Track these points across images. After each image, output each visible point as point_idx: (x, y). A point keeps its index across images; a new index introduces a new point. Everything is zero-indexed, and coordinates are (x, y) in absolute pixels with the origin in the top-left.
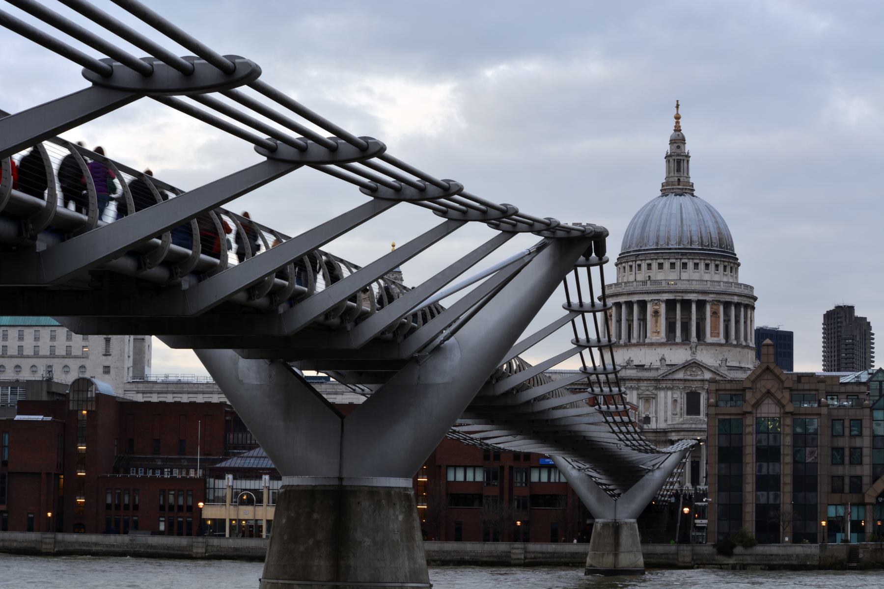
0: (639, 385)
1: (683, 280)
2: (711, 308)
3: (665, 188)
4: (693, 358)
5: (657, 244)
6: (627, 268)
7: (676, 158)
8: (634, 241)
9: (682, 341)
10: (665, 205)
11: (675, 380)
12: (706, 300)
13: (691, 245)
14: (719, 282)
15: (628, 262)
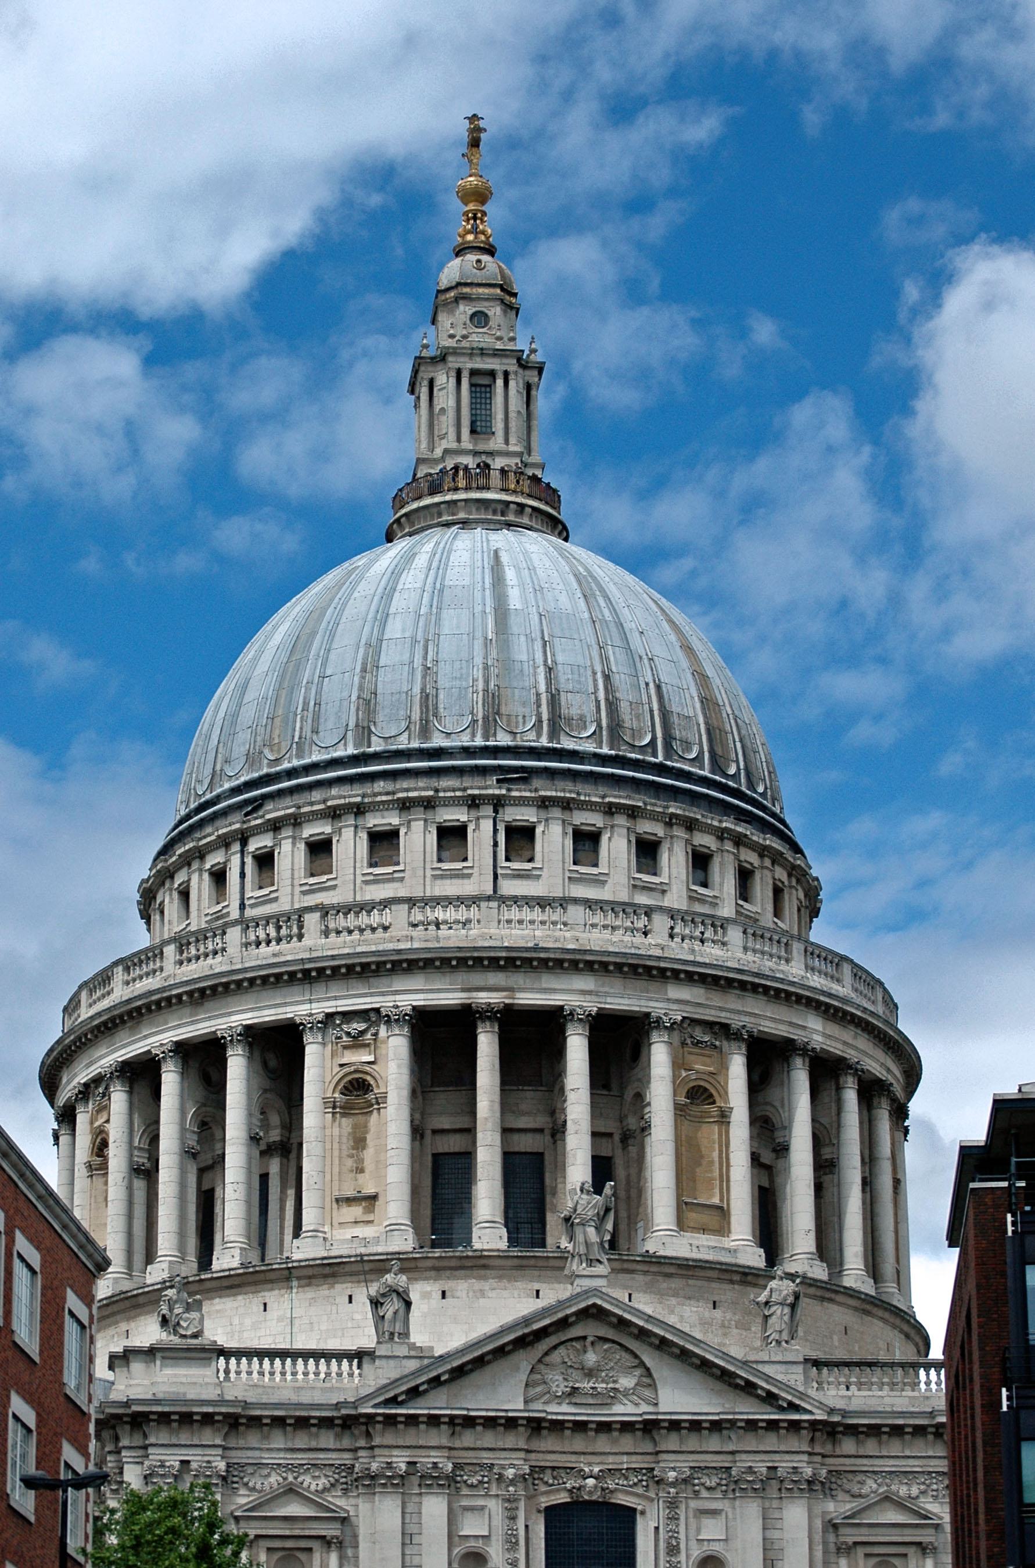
0: (239, 1457)
1: (516, 900)
2: (677, 1064)
3: (415, 505)
4: (587, 1283)
5: (364, 732)
6: (200, 885)
7: (468, 365)
8: (239, 750)
9: (512, 1241)
10: (409, 557)
11: (469, 1422)
12: (647, 1015)
13: (553, 735)
14: (720, 924)
15: (201, 854)
